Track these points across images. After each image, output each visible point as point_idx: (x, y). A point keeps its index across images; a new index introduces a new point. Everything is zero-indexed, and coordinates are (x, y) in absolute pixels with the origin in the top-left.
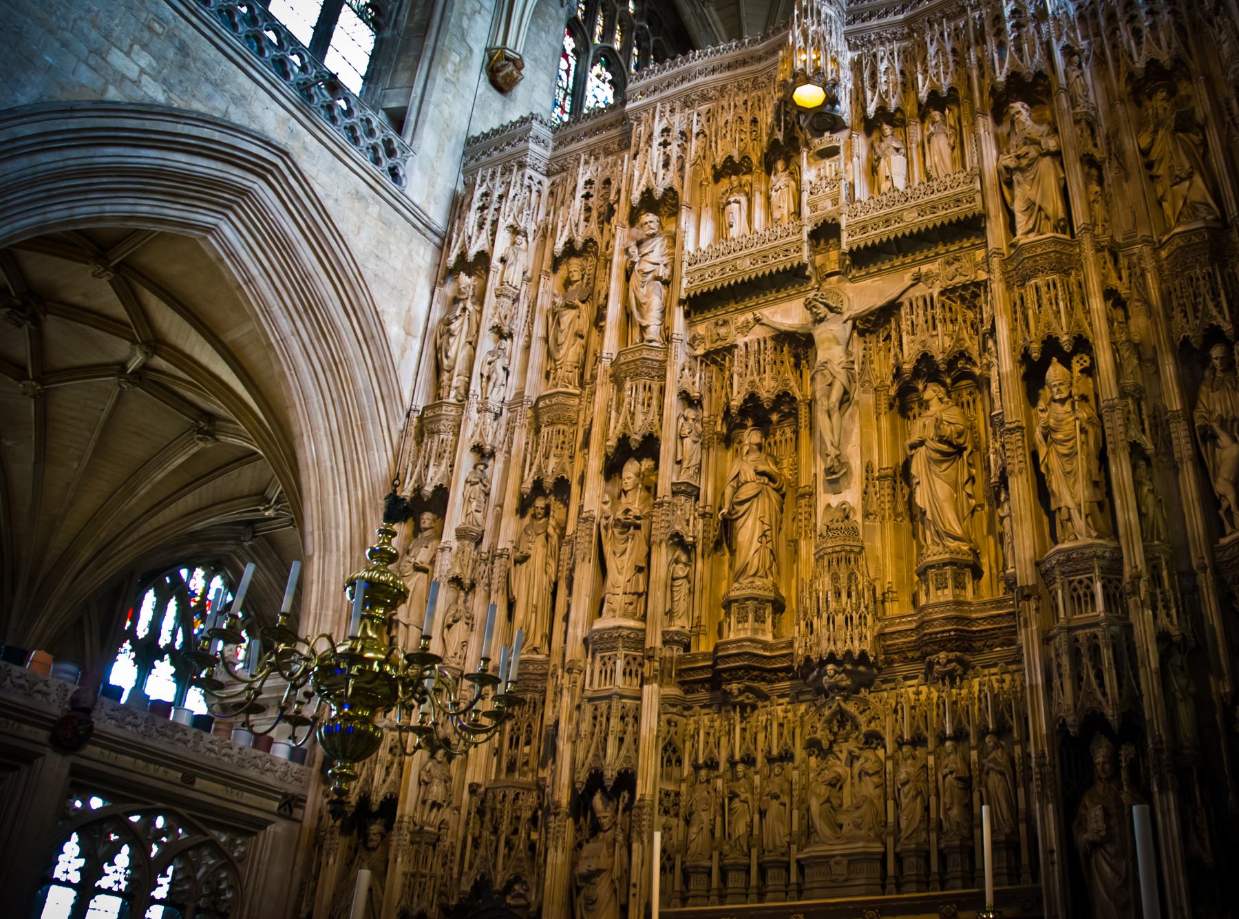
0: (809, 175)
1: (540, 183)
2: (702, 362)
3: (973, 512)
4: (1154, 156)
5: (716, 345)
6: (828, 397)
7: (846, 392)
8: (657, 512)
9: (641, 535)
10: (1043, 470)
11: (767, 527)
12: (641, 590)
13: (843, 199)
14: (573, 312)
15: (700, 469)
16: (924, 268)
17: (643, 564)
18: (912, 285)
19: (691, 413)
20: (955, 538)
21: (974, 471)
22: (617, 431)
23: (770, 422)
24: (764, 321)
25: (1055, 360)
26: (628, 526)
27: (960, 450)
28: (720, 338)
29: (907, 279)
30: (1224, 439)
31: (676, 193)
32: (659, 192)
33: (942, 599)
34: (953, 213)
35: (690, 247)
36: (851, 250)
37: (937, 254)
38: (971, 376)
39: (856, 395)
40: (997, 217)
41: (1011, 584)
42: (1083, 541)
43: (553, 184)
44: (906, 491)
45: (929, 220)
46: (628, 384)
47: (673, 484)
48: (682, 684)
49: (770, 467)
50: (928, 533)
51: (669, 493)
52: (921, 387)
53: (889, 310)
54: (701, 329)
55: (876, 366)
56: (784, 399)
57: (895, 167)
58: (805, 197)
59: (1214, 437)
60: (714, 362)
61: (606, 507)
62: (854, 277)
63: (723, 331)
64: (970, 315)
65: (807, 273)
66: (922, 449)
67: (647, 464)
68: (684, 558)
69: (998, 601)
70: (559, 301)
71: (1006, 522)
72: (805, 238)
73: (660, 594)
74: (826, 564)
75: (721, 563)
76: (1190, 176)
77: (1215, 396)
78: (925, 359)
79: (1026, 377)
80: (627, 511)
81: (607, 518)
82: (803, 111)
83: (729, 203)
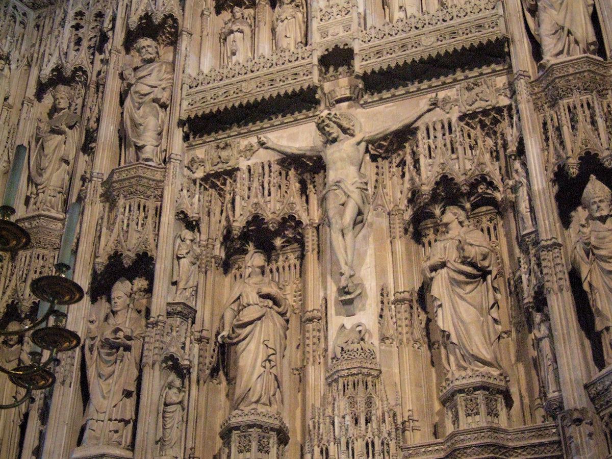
1: (24, 14)
2: (201, 185)
3: (499, 338)
5: (216, 168)
6: (342, 216)
7: (360, 213)
8: (152, 332)
9: (130, 358)
10: (586, 287)
11: (271, 352)
12: (127, 418)
13: (355, 26)
14: (59, 138)
15: (196, 291)
16: (442, 95)
17: (132, 388)
18: (429, 110)
19: (188, 234)
20: (485, 363)
21: (499, 296)
22: (108, 249)
23: (274, 248)
24: (269, 145)
25: (593, 177)
26: (114, 347)
28: (221, 160)
29: (423, 103)
31: (175, 20)
32: (157, 19)
33: (474, 426)
34: (476, 38)
35: (192, 71)
36: (365, 73)
37: (455, 80)
38: (492, 202)
39: (370, 216)
40: (522, 41)
41: (555, 410)
43: (39, 17)
44: (423, 317)
45: (450, 44)
46: (121, 201)
47: (169, 304)
49: (273, 290)
50: (452, 358)
51: (164, 313)
52: (437, 212)
53: (406, 134)
54: (200, 153)
55: (388, 190)
56: (290, 222)
58: (315, 24)
60: (214, 186)
61: (92, 327)
62: (366, 103)
63: (224, 154)
64: (490, 142)
65: (317, 97)
67: (140, 283)
68: (178, 382)
69: (539, 429)
70: (45, 127)
71: (545, 344)
72: (315, 61)
73: (151, 419)
74: (341, 387)
75: (217, 392)
78: (445, 181)
79: (558, 197)
80: (117, 330)
81: (93, 339)
83: (232, 32)
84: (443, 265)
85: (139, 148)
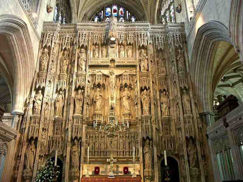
0: (110, 50)
4: (159, 62)
7: (114, 86)
14: (66, 61)
17: (82, 106)
20: (129, 110)
27: (130, 98)
30: (164, 104)
34: (133, 64)
38: (131, 87)
39: (115, 87)
42: (147, 115)
48: (87, 125)
54: (90, 70)
57: (122, 53)
59: (163, 103)
63: (95, 72)
66: (125, 97)
76: (163, 67)
77: (164, 98)
82: (111, 41)
84: (125, 96)
85: (82, 68)
